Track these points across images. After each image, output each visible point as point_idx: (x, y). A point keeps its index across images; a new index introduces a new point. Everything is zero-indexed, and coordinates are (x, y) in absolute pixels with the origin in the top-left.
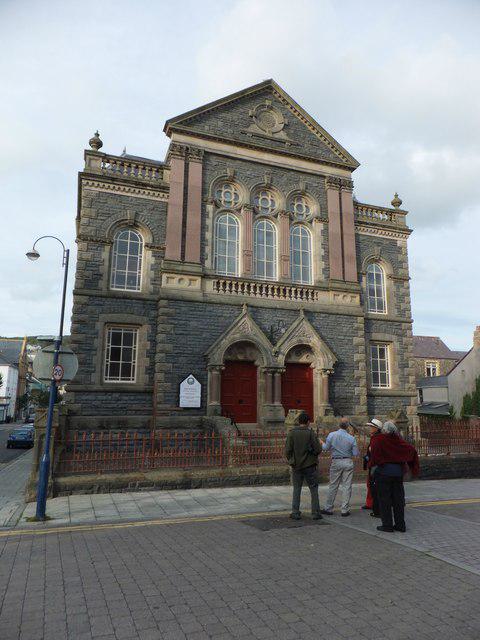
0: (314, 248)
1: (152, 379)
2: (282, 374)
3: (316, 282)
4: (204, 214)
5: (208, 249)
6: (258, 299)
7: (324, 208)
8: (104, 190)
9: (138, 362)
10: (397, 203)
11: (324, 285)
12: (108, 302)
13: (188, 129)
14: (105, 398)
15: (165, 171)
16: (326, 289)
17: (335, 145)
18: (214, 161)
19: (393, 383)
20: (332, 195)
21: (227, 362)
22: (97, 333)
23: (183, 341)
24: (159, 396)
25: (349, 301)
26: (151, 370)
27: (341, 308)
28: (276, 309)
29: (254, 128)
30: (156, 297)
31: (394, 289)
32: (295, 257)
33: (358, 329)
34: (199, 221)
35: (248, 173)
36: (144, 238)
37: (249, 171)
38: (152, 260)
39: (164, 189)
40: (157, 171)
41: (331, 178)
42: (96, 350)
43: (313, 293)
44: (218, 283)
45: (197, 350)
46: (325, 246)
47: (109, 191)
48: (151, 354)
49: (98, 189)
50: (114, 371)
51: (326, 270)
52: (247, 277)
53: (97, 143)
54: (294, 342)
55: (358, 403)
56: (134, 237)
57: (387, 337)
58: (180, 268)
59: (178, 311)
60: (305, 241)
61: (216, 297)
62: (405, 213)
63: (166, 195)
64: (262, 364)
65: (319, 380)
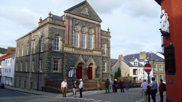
0: (93, 41)
1: (62, 71)
4: (72, 33)
5: (73, 41)
9: (59, 67)
10: (108, 30)
13: (70, 12)
15: (64, 22)
16: (95, 50)
17: (98, 16)
18: (74, 19)
20: (97, 28)
21: (78, 67)
24: (64, 75)
25: (99, 53)
26: (62, 69)
29: (82, 12)
32: (89, 43)
38: (62, 44)
39: (65, 27)
46: (95, 40)
47: (54, 27)
48: (62, 65)
50: (55, 70)
51: (95, 46)
53: (50, 14)
54: (90, 63)
56: (58, 38)
57: (106, 61)
58: (68, 46)
60: (91, 39)
64: (83, 68)
65: (94, 71)
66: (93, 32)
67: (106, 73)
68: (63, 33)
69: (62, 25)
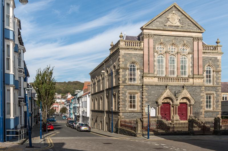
4: (154, 57)
6: (171, 83)
9: (138, 104)
12: (129, 87)
14: (130, 114)
16: (193, 78)
22: (126, 96)
23: (150, 97)
27: (197, 84)
29: (169, 23)
31: (215, 75)
35: (167, 40)
37: (167, 39)
38: (139, 73)
39: (142, 49)
40: (139, 43)
41: (195, 37)
42: (126, 101)
43: (187, 79)
44: (159, 79)
45: (154, 100)
49: (124, 52)
50: (131, 107)
51: (193, 71)
57: (212, 92)
58: (148, 75)
59: (148, 88)
61: (158, 83)
63: (143, 51)
66: (188, 50)
69: (138, 48)
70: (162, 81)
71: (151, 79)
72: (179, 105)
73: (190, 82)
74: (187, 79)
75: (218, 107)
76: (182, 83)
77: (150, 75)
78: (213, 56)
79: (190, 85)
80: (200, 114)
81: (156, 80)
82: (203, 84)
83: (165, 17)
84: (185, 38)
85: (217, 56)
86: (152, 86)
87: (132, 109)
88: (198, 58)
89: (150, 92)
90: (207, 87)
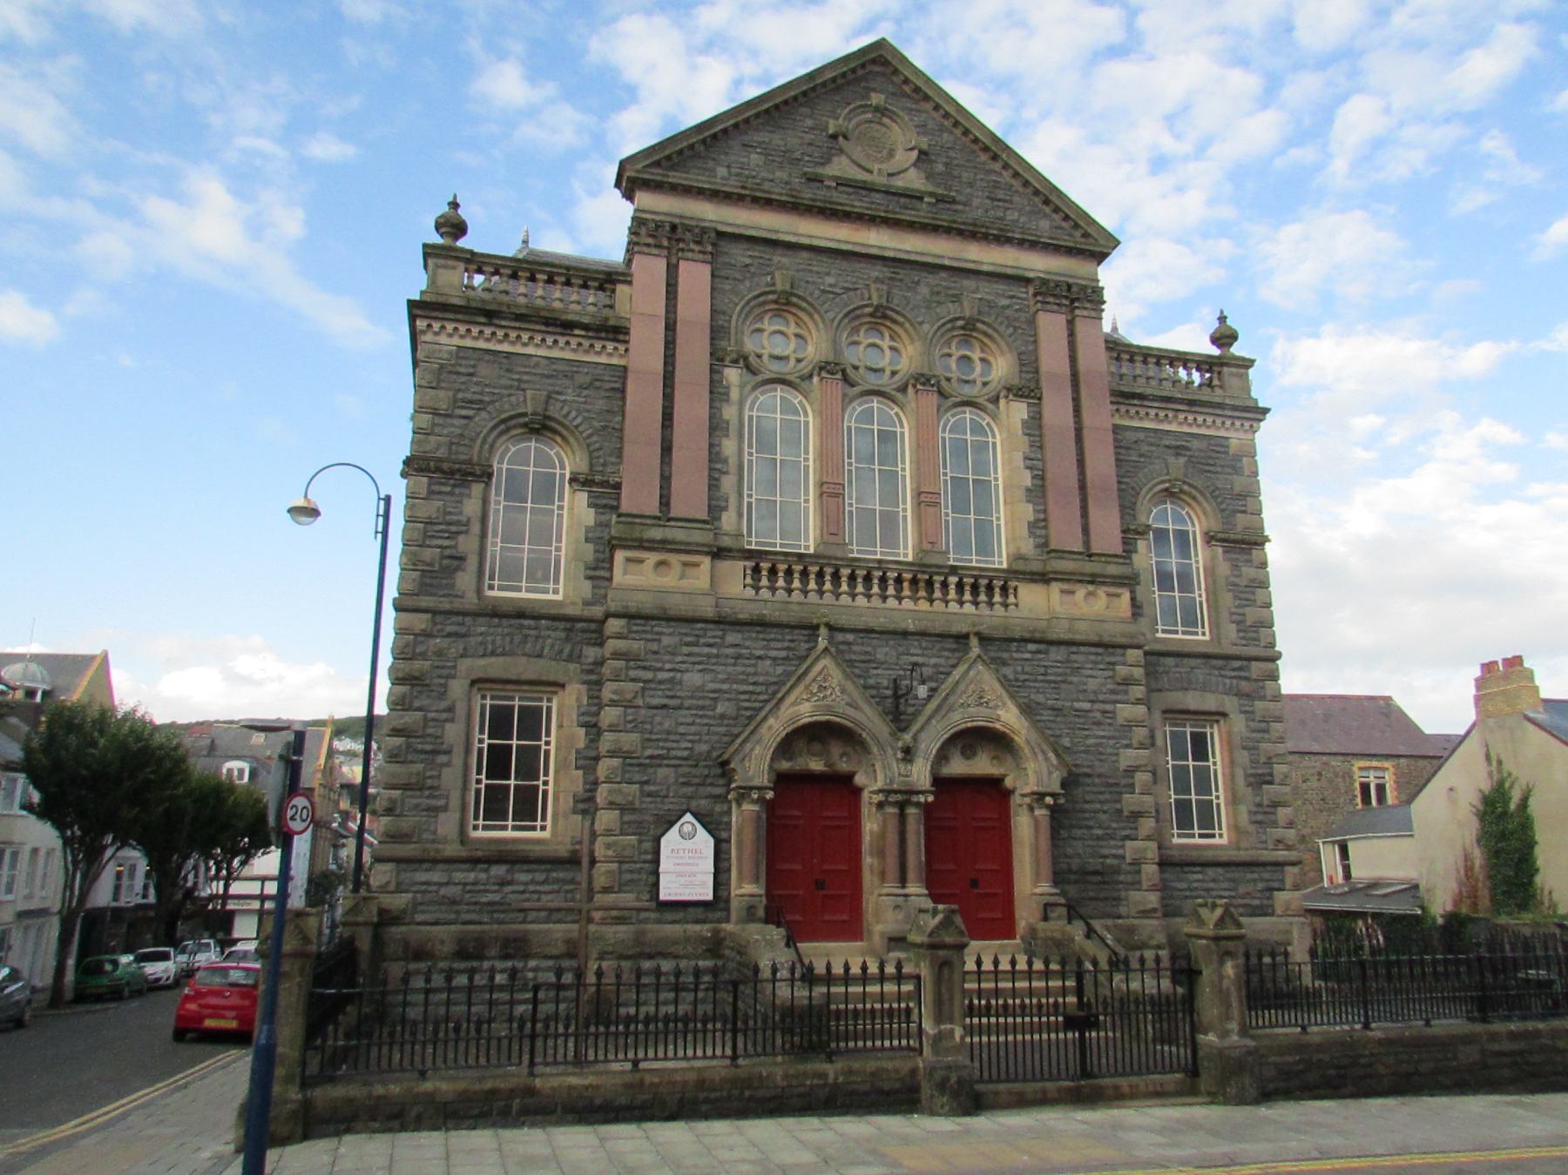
2: (927, 809)
3: (1017, 557)
4: (717, 392)
6: (861, 607)
7: (1029, 363)
8: (469, 343)
9: (558, 784)
10: (1224, 337)
11: (1036, 566)
13: (675, 177)
15: (620, 288)
16: (1043, 578)
18: (739, 255)
19: (1235, 828)
20: (1051, 325)
21: (783, 781)
22: (451, 709)
26: (586, 804)
27: (1081, 626)
28: (905, 634)
29: (840, 167)
30: (597, 611)
31: (1224, 569)
33: (1127, 682)
34: (704, 412)
35: (830, 280)
36: (567, 461)
37: (832, 276)
38: (589, 517)
39: (616, 332)
41: (1044, 282)
42: (449, 752)
43: (1004, 589)
44: (756, 570)
45: (704, 748)
46: (1037, 464)
47: (481, 344)
48: (588, 761)
49: (456, 341)
50: (494, 807)
51: (1039, 526)
52: (833, 552)
53: (453, 226)
54: (959, 720)
55: (1136, 884)
57: (1210, 702)
58: (657, 534)
59: (654, 647)
62: (1248, 363)
63: (622, 348)
64: (873, 780)
66: (1002, 368)
67: (1224, 856)
68: (600, 404)
70: (790, 591)
71: (685, 564)
72: (931, 798)
73: (1024, 613)
74: (1004, 589)
75: (1274, 824)
76: (961, 613)
77: (678, 534)
78: (1195, 430)
79: (1027, 635)
80: (1122, 878)
81: (734, 582)
82: (1132, 628)
83: (809, 122)
84: (969, 283)
85: (1222, 433)
86: (684, 628)
87: (509, 834)
88: (1079, 431)
89: (662, 675)
90: (1170, 661)
